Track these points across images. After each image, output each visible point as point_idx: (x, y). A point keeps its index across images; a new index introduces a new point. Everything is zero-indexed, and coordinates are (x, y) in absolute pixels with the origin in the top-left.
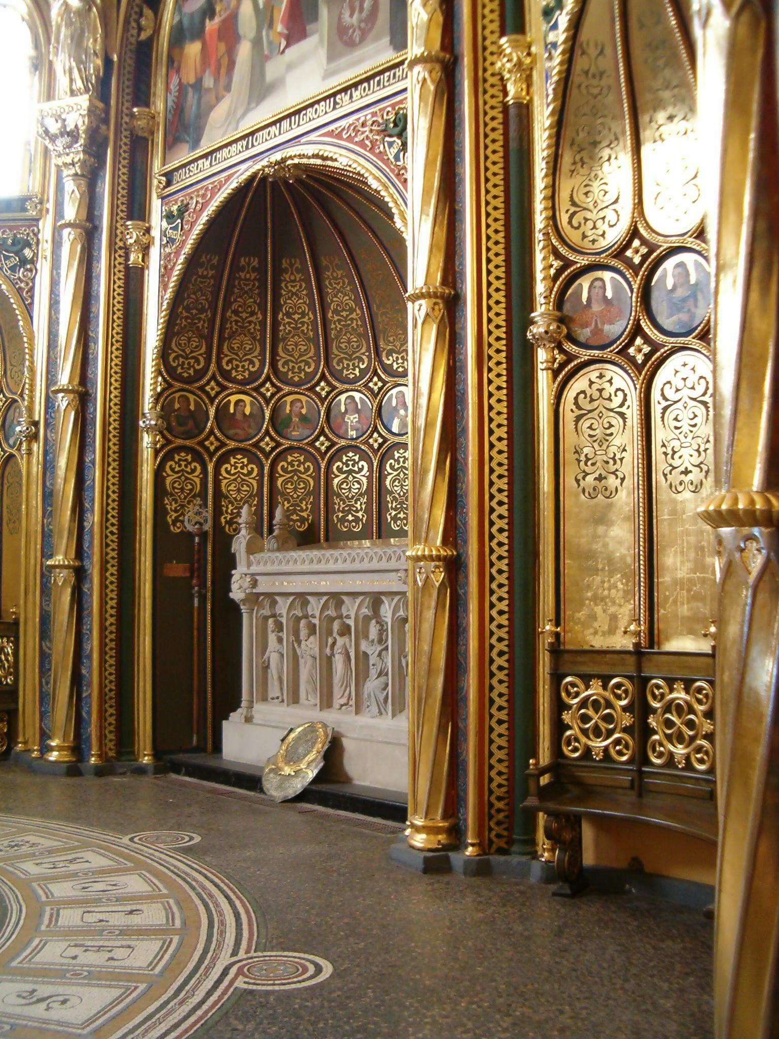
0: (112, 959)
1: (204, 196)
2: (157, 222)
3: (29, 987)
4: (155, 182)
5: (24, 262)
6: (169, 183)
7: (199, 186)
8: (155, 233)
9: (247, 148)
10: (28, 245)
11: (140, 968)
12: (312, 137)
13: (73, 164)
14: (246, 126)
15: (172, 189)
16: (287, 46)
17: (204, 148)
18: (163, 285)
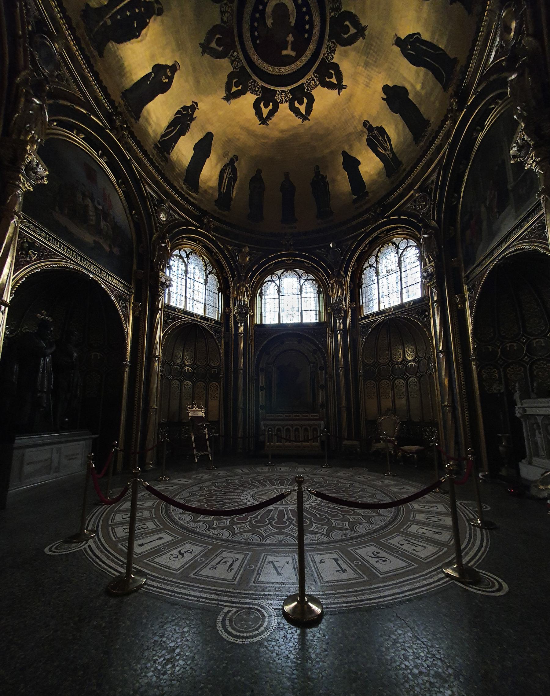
0: (414, 550)
1: (479, 279)
2: (467, 293)
3: (379, 551)
4: (464, 280)
5: (426, 316)
6: (468, 279)
7: (477, 277)
8: (467, 296)
9: (491, 257)
10: (427, 311)
11: (421, 558)
12: (514, 244)
13: (433, 283)
14: (488, 251)
15: (469, 280)
16: (499, 216)
17: (477, 263)
18: (471, 313)
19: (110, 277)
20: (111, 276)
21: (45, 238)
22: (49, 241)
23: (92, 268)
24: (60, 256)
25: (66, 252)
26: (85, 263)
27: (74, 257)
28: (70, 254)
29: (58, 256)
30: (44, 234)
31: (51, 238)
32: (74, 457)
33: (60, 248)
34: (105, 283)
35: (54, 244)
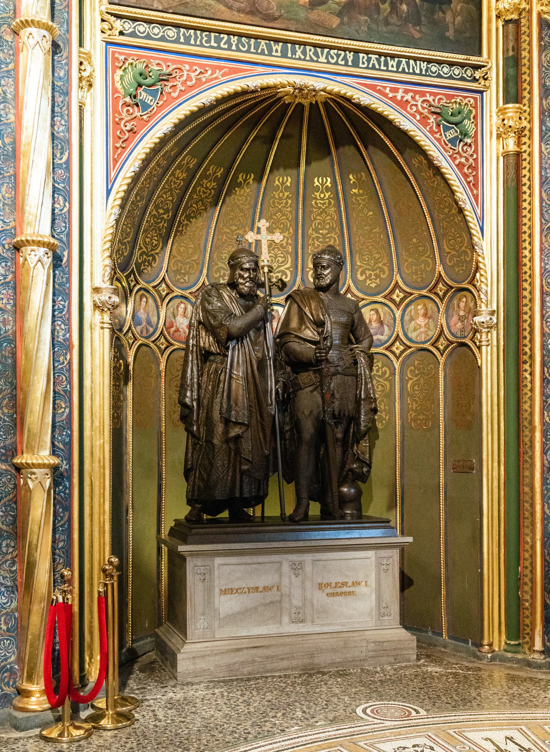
19: (391, 63)
20: (393, 57)
21: (177, 41)
22: (187, 42)
23: (323, 59)
24: (221, 68)
25: (238, 50)
26: (299, 53)
27: (263, 53)
28: (248, 51)
29: (214, 69)
30: (172, 32)
31: (192, 31)
32: (345, 589)
33: (219, 48)
34: (373, 88)
35: (202, 45)
